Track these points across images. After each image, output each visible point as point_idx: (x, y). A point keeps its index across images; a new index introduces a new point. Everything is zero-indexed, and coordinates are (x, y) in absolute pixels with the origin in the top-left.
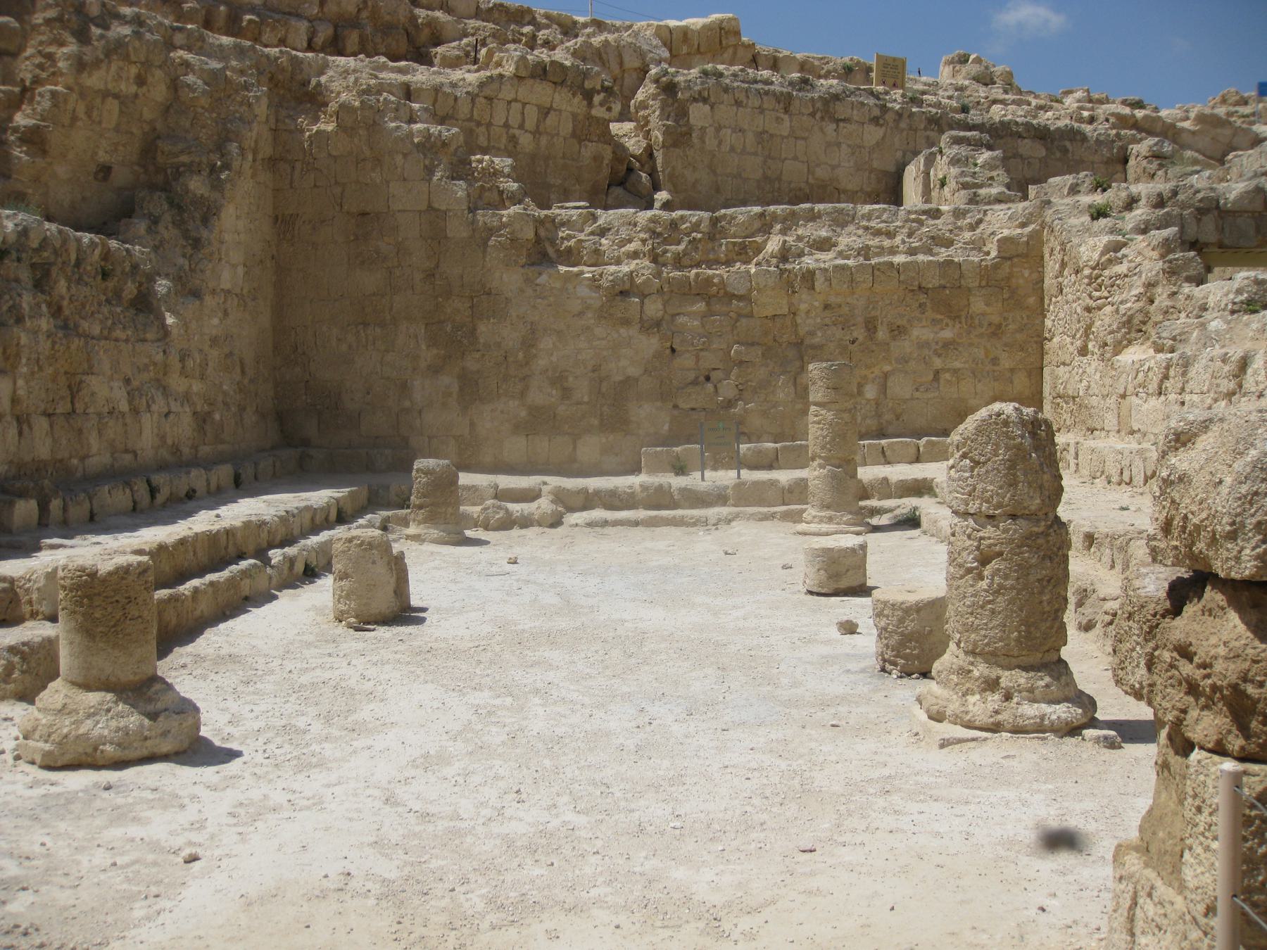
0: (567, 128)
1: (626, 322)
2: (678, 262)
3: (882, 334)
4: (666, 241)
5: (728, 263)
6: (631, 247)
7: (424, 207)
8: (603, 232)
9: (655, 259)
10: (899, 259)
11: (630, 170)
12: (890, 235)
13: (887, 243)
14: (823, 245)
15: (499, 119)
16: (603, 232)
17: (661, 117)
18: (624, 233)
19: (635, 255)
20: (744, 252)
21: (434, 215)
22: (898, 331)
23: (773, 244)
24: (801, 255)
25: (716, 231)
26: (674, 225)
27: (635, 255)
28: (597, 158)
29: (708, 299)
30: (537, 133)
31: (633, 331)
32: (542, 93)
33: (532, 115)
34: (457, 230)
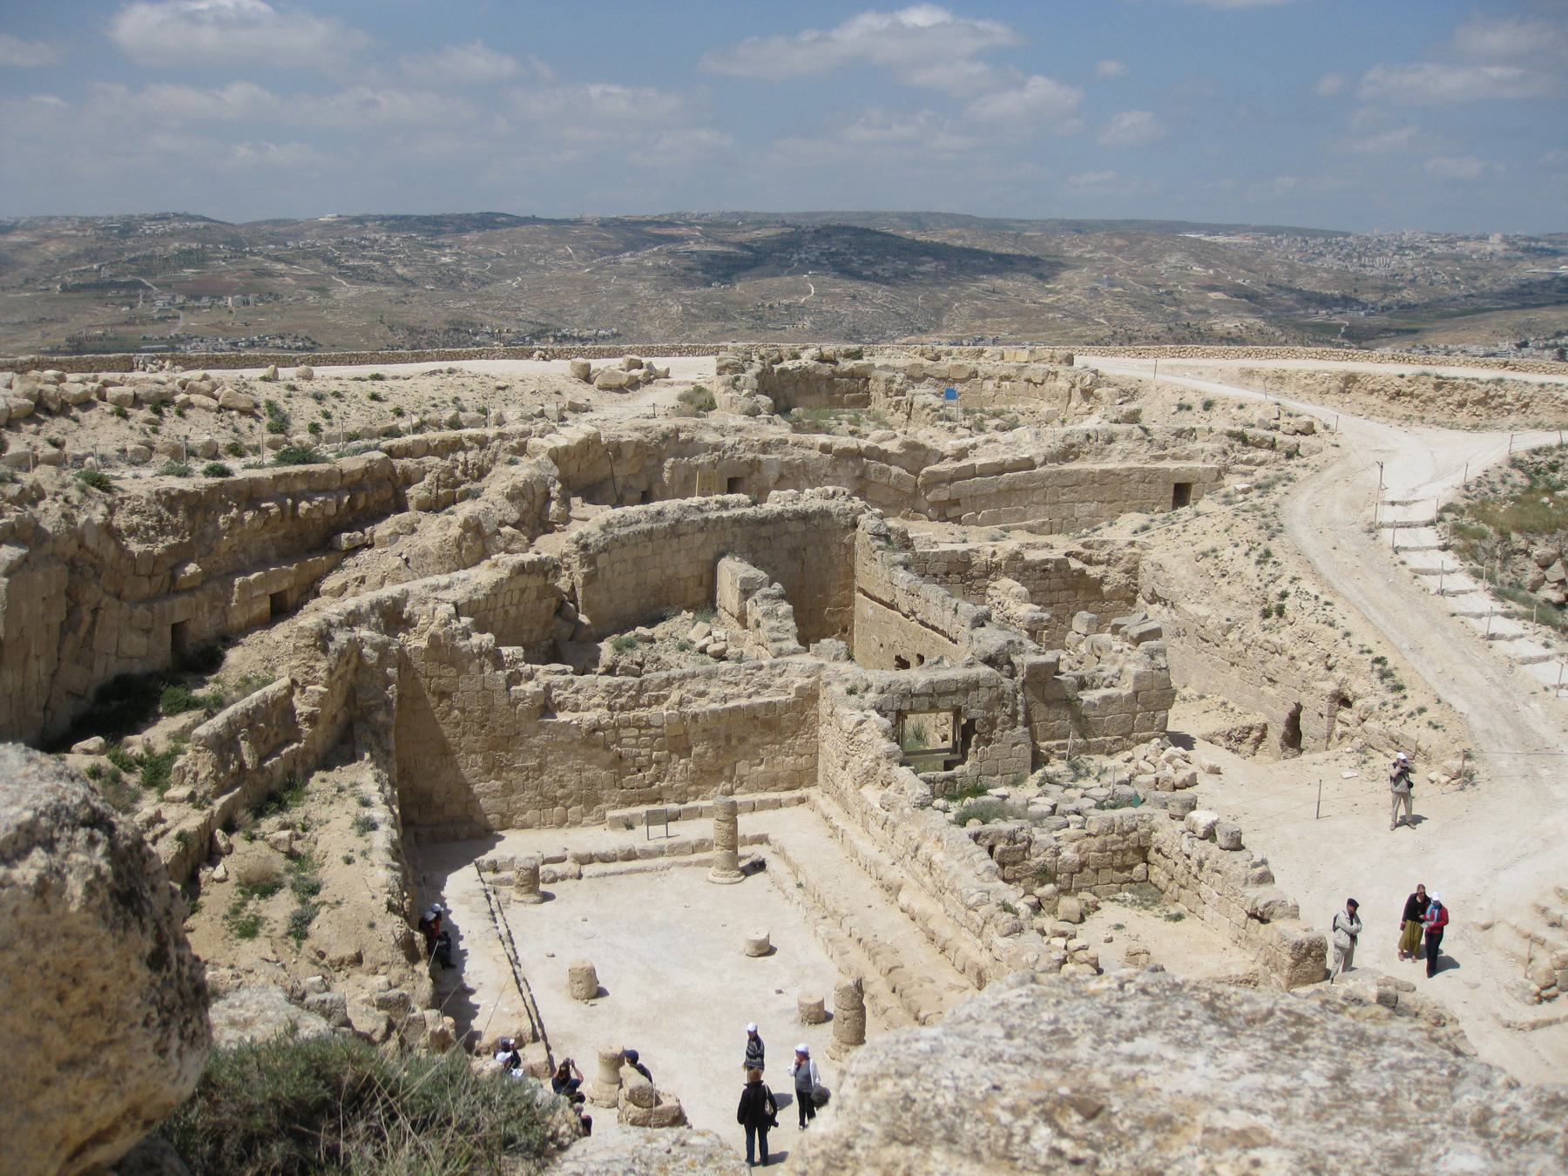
0: (534, 595)
1: (596, 746)
2: (622, 708)
3: (734, 742)
4: (617, 697)
5: (650, 706)
6: (596, 700)
7: (479, 688)
8: (577, 691)
9: (610, 708)
10: (744, 702)
11: (563, 602)
12: (737, 684)
13: (735, 690)
14: (702, 694)
15: (500, 604)
16: (577, 691)
17: (582, 565)
18: (590, 692)
19: (599, 706)
20: (658, 700)
21: (486, 693)
22: (742, 740)
23: (675, 696)
24: (690, 702)
25: (641, 690)
26: (619, 686)
27: (599, 706)
28: (548, 607)
29: (640, 728)
30: (518, 605)
31: (600, 750)
32: (523, 581)
33: (516, 594)
34: (501, 701)
